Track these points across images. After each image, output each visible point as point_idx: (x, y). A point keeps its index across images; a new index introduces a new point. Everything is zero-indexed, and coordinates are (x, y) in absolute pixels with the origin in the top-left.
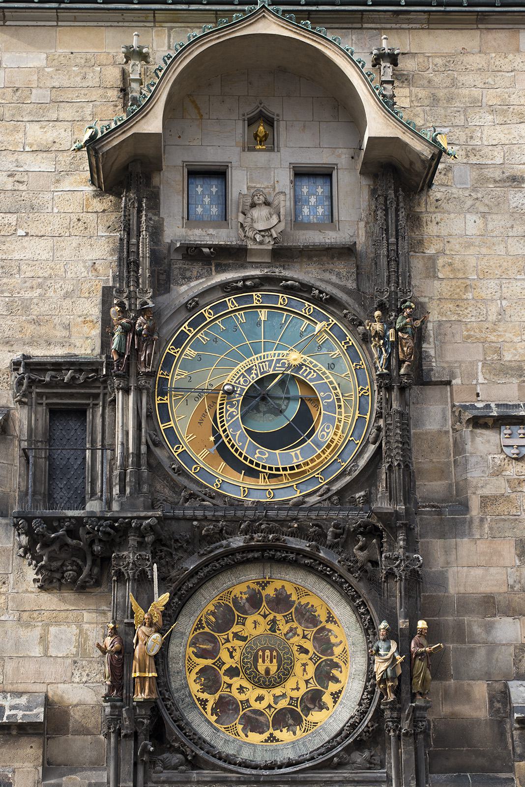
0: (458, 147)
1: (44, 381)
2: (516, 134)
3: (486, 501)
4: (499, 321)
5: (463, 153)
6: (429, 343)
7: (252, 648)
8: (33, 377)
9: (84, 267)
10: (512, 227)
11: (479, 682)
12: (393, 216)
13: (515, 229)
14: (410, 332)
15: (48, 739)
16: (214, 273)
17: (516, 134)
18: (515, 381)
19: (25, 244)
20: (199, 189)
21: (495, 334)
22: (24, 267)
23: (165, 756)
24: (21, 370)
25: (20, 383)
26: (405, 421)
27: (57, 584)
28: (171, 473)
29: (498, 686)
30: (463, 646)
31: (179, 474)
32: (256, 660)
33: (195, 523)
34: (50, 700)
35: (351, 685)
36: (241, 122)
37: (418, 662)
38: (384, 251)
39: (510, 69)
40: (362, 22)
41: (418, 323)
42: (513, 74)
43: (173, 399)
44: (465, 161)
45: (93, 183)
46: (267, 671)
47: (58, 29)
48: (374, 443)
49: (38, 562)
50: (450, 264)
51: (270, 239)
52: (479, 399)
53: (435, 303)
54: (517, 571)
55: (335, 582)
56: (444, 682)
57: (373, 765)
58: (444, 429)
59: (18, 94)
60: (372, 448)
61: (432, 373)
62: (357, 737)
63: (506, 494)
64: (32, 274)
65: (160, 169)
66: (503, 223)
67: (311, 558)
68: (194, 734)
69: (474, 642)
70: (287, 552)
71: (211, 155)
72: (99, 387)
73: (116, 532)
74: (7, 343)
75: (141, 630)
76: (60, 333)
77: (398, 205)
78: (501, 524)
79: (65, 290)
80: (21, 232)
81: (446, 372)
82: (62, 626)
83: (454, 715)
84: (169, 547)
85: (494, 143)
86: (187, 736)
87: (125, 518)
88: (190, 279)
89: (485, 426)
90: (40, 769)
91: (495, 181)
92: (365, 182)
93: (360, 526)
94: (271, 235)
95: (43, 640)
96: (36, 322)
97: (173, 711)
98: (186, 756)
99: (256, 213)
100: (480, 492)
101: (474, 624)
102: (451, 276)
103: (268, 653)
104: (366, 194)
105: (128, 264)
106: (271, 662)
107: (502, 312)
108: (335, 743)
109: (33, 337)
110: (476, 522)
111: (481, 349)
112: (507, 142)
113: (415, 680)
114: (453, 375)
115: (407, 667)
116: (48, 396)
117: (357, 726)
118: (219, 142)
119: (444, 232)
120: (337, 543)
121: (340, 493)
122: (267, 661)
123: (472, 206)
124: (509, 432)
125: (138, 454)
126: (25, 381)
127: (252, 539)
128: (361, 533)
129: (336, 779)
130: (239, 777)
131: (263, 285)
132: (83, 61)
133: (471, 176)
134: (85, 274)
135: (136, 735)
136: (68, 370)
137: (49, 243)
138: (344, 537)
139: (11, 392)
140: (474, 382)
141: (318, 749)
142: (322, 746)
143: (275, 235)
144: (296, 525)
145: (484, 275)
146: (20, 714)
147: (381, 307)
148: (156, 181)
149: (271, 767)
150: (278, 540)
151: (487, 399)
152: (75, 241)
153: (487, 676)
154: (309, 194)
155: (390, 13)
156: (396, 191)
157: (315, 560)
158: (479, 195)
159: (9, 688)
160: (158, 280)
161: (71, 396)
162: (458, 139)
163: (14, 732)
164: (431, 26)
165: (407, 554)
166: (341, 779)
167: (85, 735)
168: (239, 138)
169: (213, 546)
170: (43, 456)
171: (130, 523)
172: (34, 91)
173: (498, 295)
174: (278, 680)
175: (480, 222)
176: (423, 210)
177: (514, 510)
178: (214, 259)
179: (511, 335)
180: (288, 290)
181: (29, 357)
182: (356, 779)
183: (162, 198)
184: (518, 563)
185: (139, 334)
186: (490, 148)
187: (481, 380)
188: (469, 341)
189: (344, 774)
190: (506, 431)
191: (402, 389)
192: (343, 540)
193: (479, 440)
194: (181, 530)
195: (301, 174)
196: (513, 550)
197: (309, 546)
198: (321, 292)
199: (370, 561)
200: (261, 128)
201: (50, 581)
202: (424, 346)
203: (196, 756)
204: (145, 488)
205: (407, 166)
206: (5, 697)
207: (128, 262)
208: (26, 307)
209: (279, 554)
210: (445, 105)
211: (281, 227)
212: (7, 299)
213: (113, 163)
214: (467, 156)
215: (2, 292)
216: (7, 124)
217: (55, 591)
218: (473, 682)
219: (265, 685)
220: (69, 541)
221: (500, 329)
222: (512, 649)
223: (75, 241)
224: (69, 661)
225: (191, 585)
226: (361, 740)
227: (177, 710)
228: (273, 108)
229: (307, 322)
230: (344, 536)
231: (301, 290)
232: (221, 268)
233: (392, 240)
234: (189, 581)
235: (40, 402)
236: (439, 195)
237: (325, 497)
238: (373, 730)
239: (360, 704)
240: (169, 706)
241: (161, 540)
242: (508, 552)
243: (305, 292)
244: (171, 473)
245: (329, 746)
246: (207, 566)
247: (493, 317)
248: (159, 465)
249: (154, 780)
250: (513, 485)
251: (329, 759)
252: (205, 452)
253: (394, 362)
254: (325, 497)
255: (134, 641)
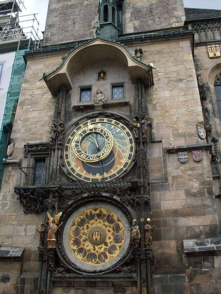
0: (162, 73)
1: (32, 150)
2: (180, 68)
3: (174, 178)
4: (177, 121)
5: (164, 74)
6: (154, 130)
7: (91, 231)
8: (29, 149)
9: (48, 117)
10: (180, 93)
11: (173, 241)
12: (140, 92)
13: (181, 94)
14: (146, 125)
15: (24, 263)
16: (85, 114)
17: (180, 68)
18: (183, 139)
19: (32, 113)
20: (84, 94)
21: (176, 125)
22: (31, 119)
23: (59, 268)
24: (27, 147)
25: (25, 151)
26: (145, 154)
27: (30, 211)
28: (67, 174)
29: (180, 242)
30: (167, 228)
31: (70, 175)
32: (93, 235)
33: (74, 190)
34: (26, 250)
35: (126, 243)
36: (96, 74)
37: (147, 233)
38: (137, 102)
39: (177, 51)
40: (132, 45)
41: (149, 122)
42: (178, 53)
43: (70, 152)
44: (164, 77)
45: (52, 95)
46: (96, 239)
47: (47, 58)
48: (134, 161)
49: (23, 204)
50: (160, 106)
51: (102, 102)
52: (171, 145)
53: (156, 117)
54: (186, 201)
55: (119, 207)
56: (160, 241)
57: (131, 272)
58: (160, 156)
59: (35, 75)
60: (133, 163)
61: (155, 139)
62: (125, 261)
63: (181, 175)
64: (33, 121)
65: (71, 89)
66: (177, 92)
67: (111, 199)
68: (69, 261)
69: (171, 227)
70: (103, 198)
71: (86, 83)
72: (49, 151)
73: (46, 193)
74: (24, 140)
75: (51, 225)
76: (39, 136)
77: (142, 89)
78: (179, 185)
79: (41, 125)
80: (31, 110)
81: (160, 138)
82: (32, 226)
83: (163, 253)
84: (64, 198)
85: (174, 70)
86: (66, 261)
87: (48, 188)
88: (77, 117)
89: (173, 153)
90: (19, 272)
91: (174, 81)
92: (133, 86)
93: (128, 188)
94: (102, 101)
95: (25, 230)
96: (33, 134)
97: (62, 253)
98: (65, 268)
99: (98, 95)
100: (171, 175)
101: (170, 220)
102: (161, 109)
103: (97, 233)
104: (134, 89)
105: (58, 113)
106: (98, 236)
107: (178, 118)
108: (118, 264)
109: (31, 138)
110: (171, 185)
111: (171, 130)
112: (177, 70)
113: (146, 240)
114: (162, 138)
115: (143, 235)
116: (35, 155)
117: (126, 257)
118: (90, 79)
119: (158, 97)
120: (121, 194)
121: (123, 178)
122: (97, 235)
123: (167, 89)
124: (180, 154)
125: (57, 170)
126: (27, 151)
127: (91, 193)
128: (129, 190)
129: (118, 277)
130: (83, 276)
131: (99, 116)
132: (53, 65)
133: (166, 81)
134: (48, 119)
135: (48, 261)
136: (40, 146)
137: (39, 112)
138: (123, 192)
139: (23, 154)
140: (169, 140)
141: (112, 266)
142: (114, 265)
143: (103, 101)
144: (107, 189)
145: (172, 108)
146: (14, 253)
147: (136, 118)
148: (70, 92)
149: (95, 272)
150: (99, 193)
151: (173, 145)
152: (46, 111)
153: (176, 239)
154: (117, 92)
155: (140, 41)
156: (141, 85)
157: (112, 200)
158: (169, 85)
159: (14, 245)
160: (69, 119)
161: (41, 154)
162: (162, 71)
163: (12, 260)
164: (153, 43)
165: (144, 196)
166: (119, 277)
167: (35, 261)
168: (95, 78)
169: (78, 197)
170: (31, 173)
171: (49, 189)
172: (39, 74)
173: (176, 113)
174: (100, 242)
175: (170, 93)
176: (152, 91)
177: (184, 180)
178: (85, 110)
179: (181, 125)
180: (107, 116)
181: (29, 144)
182: (125, 277)
183: (72, 96)
184: (186, 198)
185: (58, 132)
186: (172, 72)
187: (172, 139)
188: (167, 128)
189: (121, 275)
190: (180, 153)
191: (143, 143)
192: (123, 193)
193: (171, 158)
194: (69, 193)
195: (114, 86)
196: (184, 194)
197: (110, 195)
198: (117, 116)
199: (132, 200)
200: (102, 75)
201: (28, 210)
202: (152, 130)
203: (68, 268)
204: (58, 179)
205: (144, 77)
206: (12, 249)
207: (58, 113)
208: (30, 129)
209: (100, 198)
210: (158, 63)
211: (106, 99)
212: (25, 128)
213: (54, 85)
214: (165, 75)
215: (24, 126)
216: (31, 83)
217: (30, 214)
218: (170, 241)
219: (95, 244)
220: (31, 196)
221: (178, 123)
222: (185, 228)
223: (46, 111)
224: (33, 237)
225: (70, 210)
226: (127, 262)
227: (64, 252)
228: (105, 69)
229: (113, 126)
230: (123, 192)
231: (112, 116)
232: (87, 112)
233: (140, 98)
234: (69, 209)
235: (32, 157)
236: (156, 87)
237: (117, 179)
238: (131, 258)
239: (128, 249)
240: (60, 251)
241: (62, 196)
242: (182, 194)
243: (112, 117)
244: (67, 174)
245: (115, 265)
246: (75, 203)
247: (175, 120)
248: (63, 172)
249: (54, 277)
250: (183, 172)
251: (115, 270)
252: (79, 168)
253: (141, 134)
254: (117, 179)
255: (48, 228)
